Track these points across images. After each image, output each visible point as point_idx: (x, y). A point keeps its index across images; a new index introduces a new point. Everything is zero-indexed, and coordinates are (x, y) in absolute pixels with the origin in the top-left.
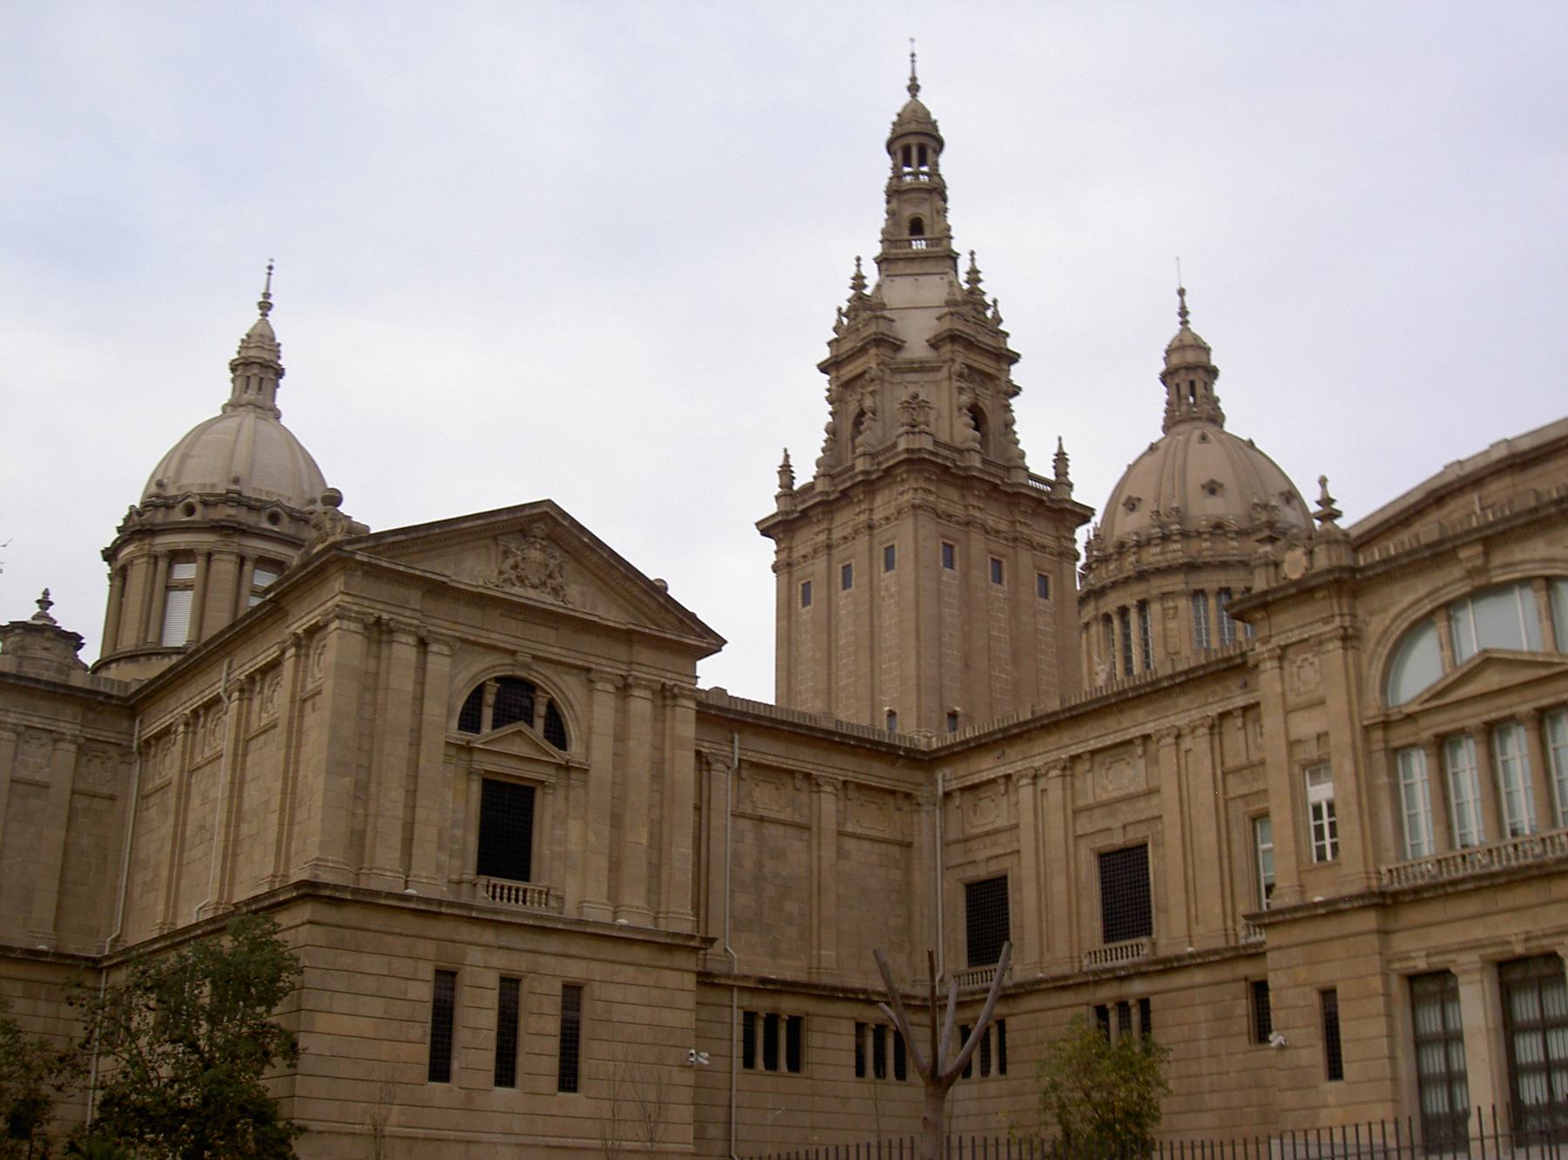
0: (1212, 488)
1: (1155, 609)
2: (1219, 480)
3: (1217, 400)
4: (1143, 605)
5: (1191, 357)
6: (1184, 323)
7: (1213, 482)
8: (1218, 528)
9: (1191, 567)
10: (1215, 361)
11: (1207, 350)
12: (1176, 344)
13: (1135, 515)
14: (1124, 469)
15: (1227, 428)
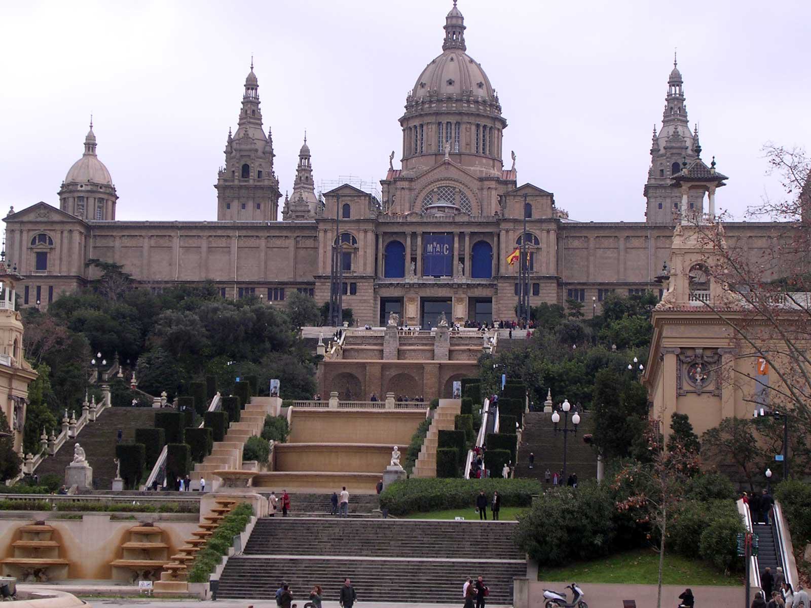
0: (450, 83)
1: (425, 128)
2: (453, 79)
3: (463, 40)
4: (422, 126)
5: (454, 21)
6: (455, 5)
7: (450, 80)
8: (449, 99)
9: (437, 114)
10: (465, 24)
11: (462, 18)
12: (450, 15)
13: (423, 90)
14: (426, 66)
15: (466, 52)
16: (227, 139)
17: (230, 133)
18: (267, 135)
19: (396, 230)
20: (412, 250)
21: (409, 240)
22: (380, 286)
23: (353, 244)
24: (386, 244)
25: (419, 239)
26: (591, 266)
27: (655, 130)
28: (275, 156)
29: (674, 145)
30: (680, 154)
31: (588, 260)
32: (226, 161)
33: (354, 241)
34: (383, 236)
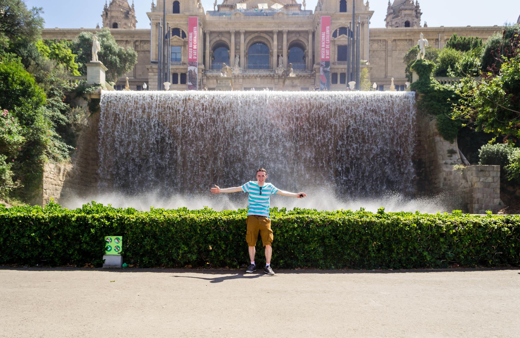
16: (103, 8)
17: (106, 4)
18: (130, 5)
19: (221, 29)
20: (236, 49)
21: (233, 37)
22: (208, 78)
23: (183, 38)
24: (212, 43)
25: (242, 37)
26: (389, 65)
27: (389, 2)
28: (137, 22)
29: (406, 7)
30: (410, 15)
31: (386, 60)
32: (103, 22)
33: (184, 36)
34: (210, 35)
